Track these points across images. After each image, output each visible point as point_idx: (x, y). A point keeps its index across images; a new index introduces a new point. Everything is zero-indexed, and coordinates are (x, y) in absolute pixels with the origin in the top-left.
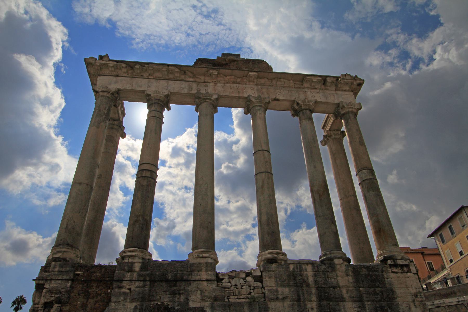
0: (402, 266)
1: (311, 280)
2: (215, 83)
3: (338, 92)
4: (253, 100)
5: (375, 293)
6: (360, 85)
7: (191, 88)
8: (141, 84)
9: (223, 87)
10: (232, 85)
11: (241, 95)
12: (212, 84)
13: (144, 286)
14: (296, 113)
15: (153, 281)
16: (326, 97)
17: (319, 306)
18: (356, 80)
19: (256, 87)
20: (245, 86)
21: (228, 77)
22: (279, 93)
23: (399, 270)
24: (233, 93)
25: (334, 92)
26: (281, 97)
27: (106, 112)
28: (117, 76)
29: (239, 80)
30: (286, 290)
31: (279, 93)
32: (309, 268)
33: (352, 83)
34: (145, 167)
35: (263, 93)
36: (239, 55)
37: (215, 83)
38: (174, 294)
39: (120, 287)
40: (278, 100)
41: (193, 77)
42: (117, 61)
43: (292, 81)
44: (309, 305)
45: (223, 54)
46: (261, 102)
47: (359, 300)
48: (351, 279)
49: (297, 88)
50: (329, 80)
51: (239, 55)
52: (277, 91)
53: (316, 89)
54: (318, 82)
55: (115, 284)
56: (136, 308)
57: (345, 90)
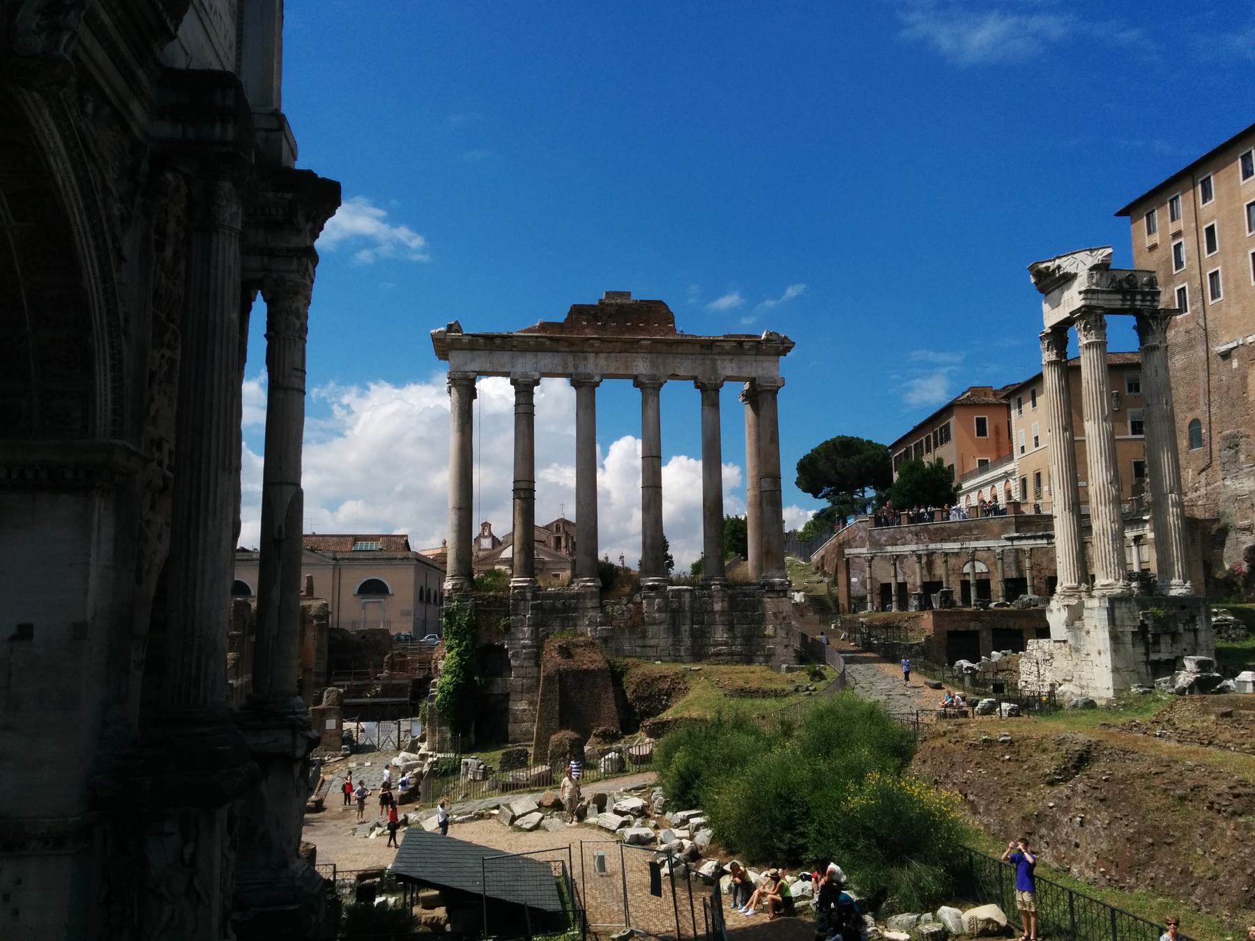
0: (779, 592)
2: (597, 353)
3: (759, 358)
6: (788, 349)
7: (565, 366)
8: (503, 358)
10: (619, 355)
11: (629, 372)
12: (592, 355)
16: (740, 368)
18: (783, 343)
19: (649, 356)
23: (775, 595)
24: (617, 369)
25: (752, 358)
28: (472, 349)
29: (627, 346)
30: (663, 615)
32: (687, 595)
34: (523, 485)
36: (629, 294)
37: (597, 353)
42: (473, 336)
43: (697, 346)
44: (683, 628)
50: (746, 346)
51: (629, 294)
53: (729, 354)
57: (768, 354)
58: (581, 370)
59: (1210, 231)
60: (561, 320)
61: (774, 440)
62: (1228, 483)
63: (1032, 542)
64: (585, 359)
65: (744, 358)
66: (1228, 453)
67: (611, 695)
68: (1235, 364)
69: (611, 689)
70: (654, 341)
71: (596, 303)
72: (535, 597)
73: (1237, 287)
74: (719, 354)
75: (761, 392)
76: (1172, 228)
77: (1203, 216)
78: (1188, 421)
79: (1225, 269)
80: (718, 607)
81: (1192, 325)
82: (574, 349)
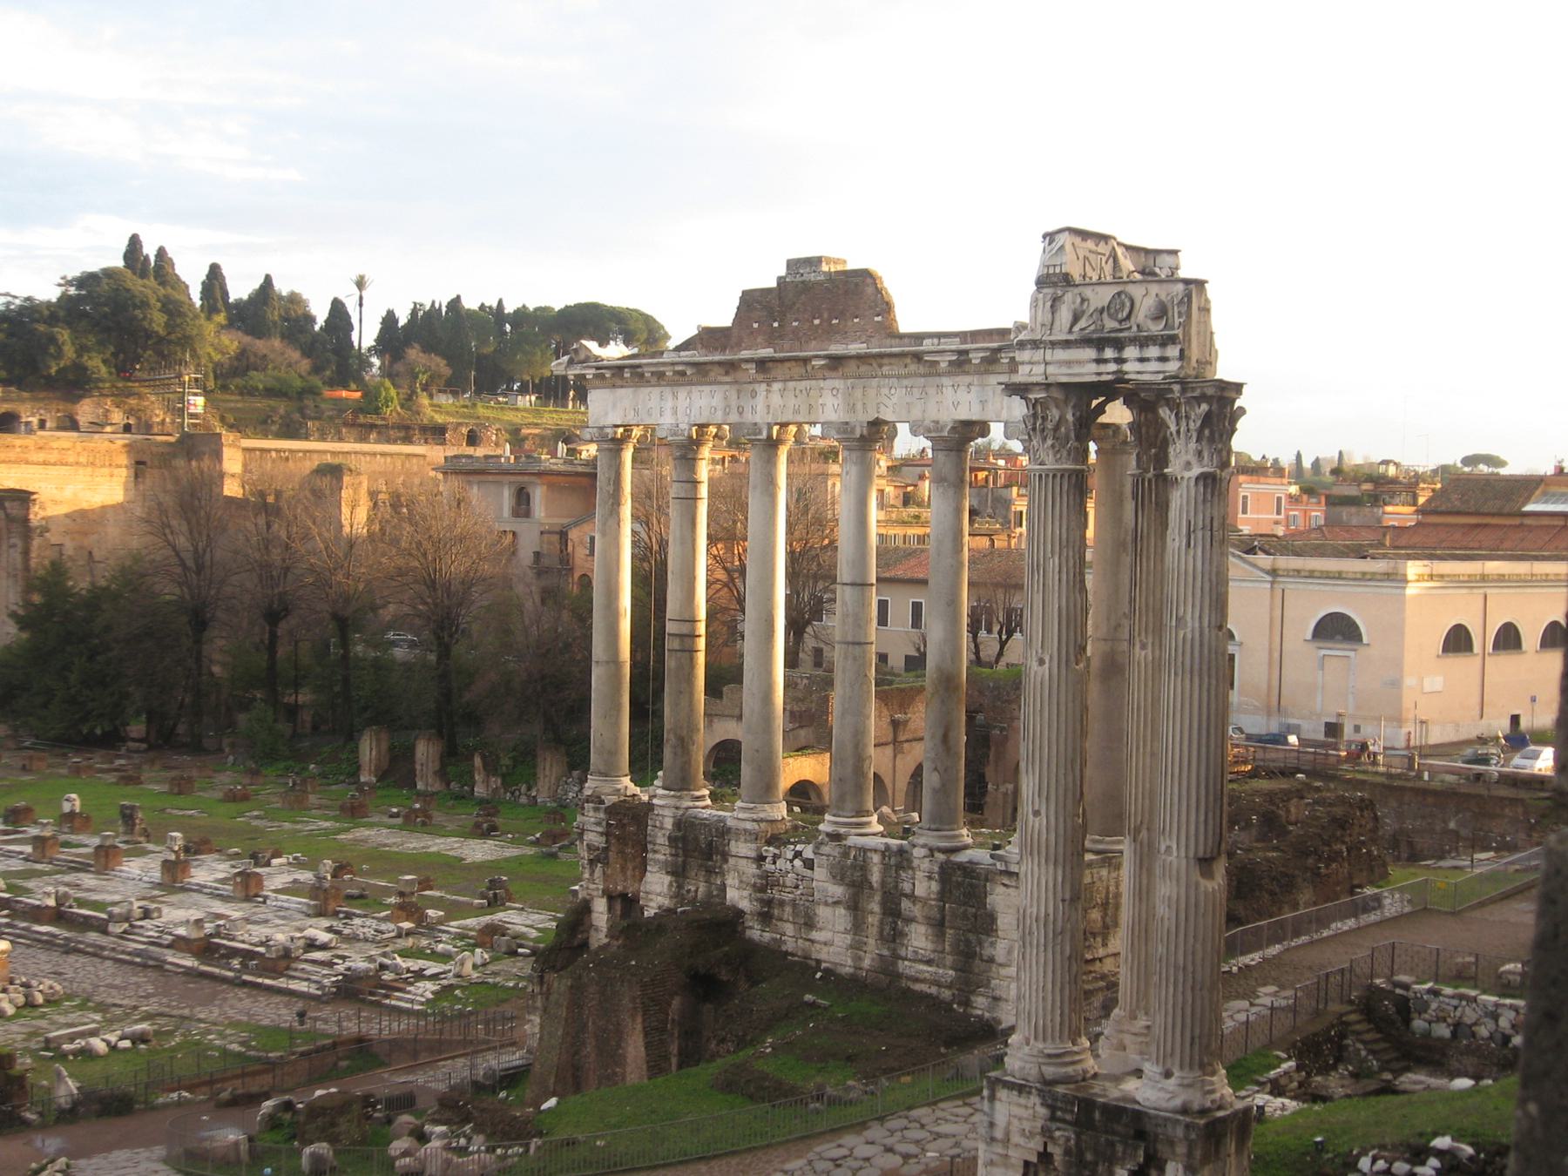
1: (875, 877)
5: (965, 916)
9: (783, 392)
12: (764, 386)
13: (676, 855)
15: (685, 851)
17: (881, 922)
19: (838, 383)
20: (822, 384)
21: (787, 365)
22: (886, 401)
24: (797, 412)
27: (611, 489)
28: (614, 386)
31: (886, 401)
32: (876, 858)
38: (710, 872)
39: (655, 852)
41: (727, 373)
43: (908, 360)
45: (793, 265)
47: (938, 926)
48: (935, 886)
49: (924, 376)
50: (976, 358)
52: (885, 391)
55: (650, 847)
56: (671, 885)
58: (749, 417)
60: (728, 323)
64: (754, 394)
67: (639, 1027)
69: (639, 1019)
70: (836, 362)
71: (774, 284)
72: (678, 824)
80: (920, 891)
82: (740, 375)
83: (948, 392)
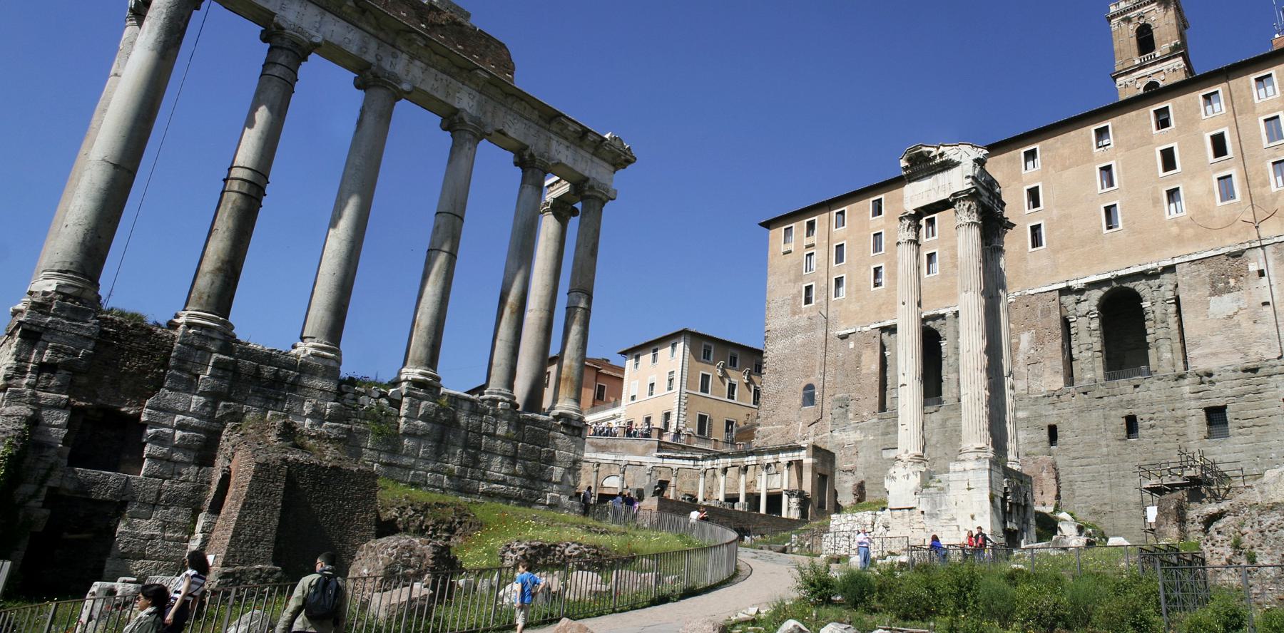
3: (595, 159)
4: (466, 119)
6: (628, 162)
14: (521, 162)
25: (588, 156)
26: (511, 133)
33: (620, 156)
35: (485, 113)
40: (504, 134)
46: (476, 129)
50: (591, 137)
53: (566, 139)
54: (576, 132)
57: (604, 160)
59: (840, 247)
61: (593, 253)
62: (835, 434)
63: (681, 462)
65: (583, 152)
66: (837, 411)
68: (852, 345)
70: (494, 82)
73: (858, 290)
74: (556, 134)
75: (589, 197)
76: (807, 241)
77: (833, 238)
78: (803, 385)
79: (849, 277)
81: (815, 314)
83: (554, 143)
